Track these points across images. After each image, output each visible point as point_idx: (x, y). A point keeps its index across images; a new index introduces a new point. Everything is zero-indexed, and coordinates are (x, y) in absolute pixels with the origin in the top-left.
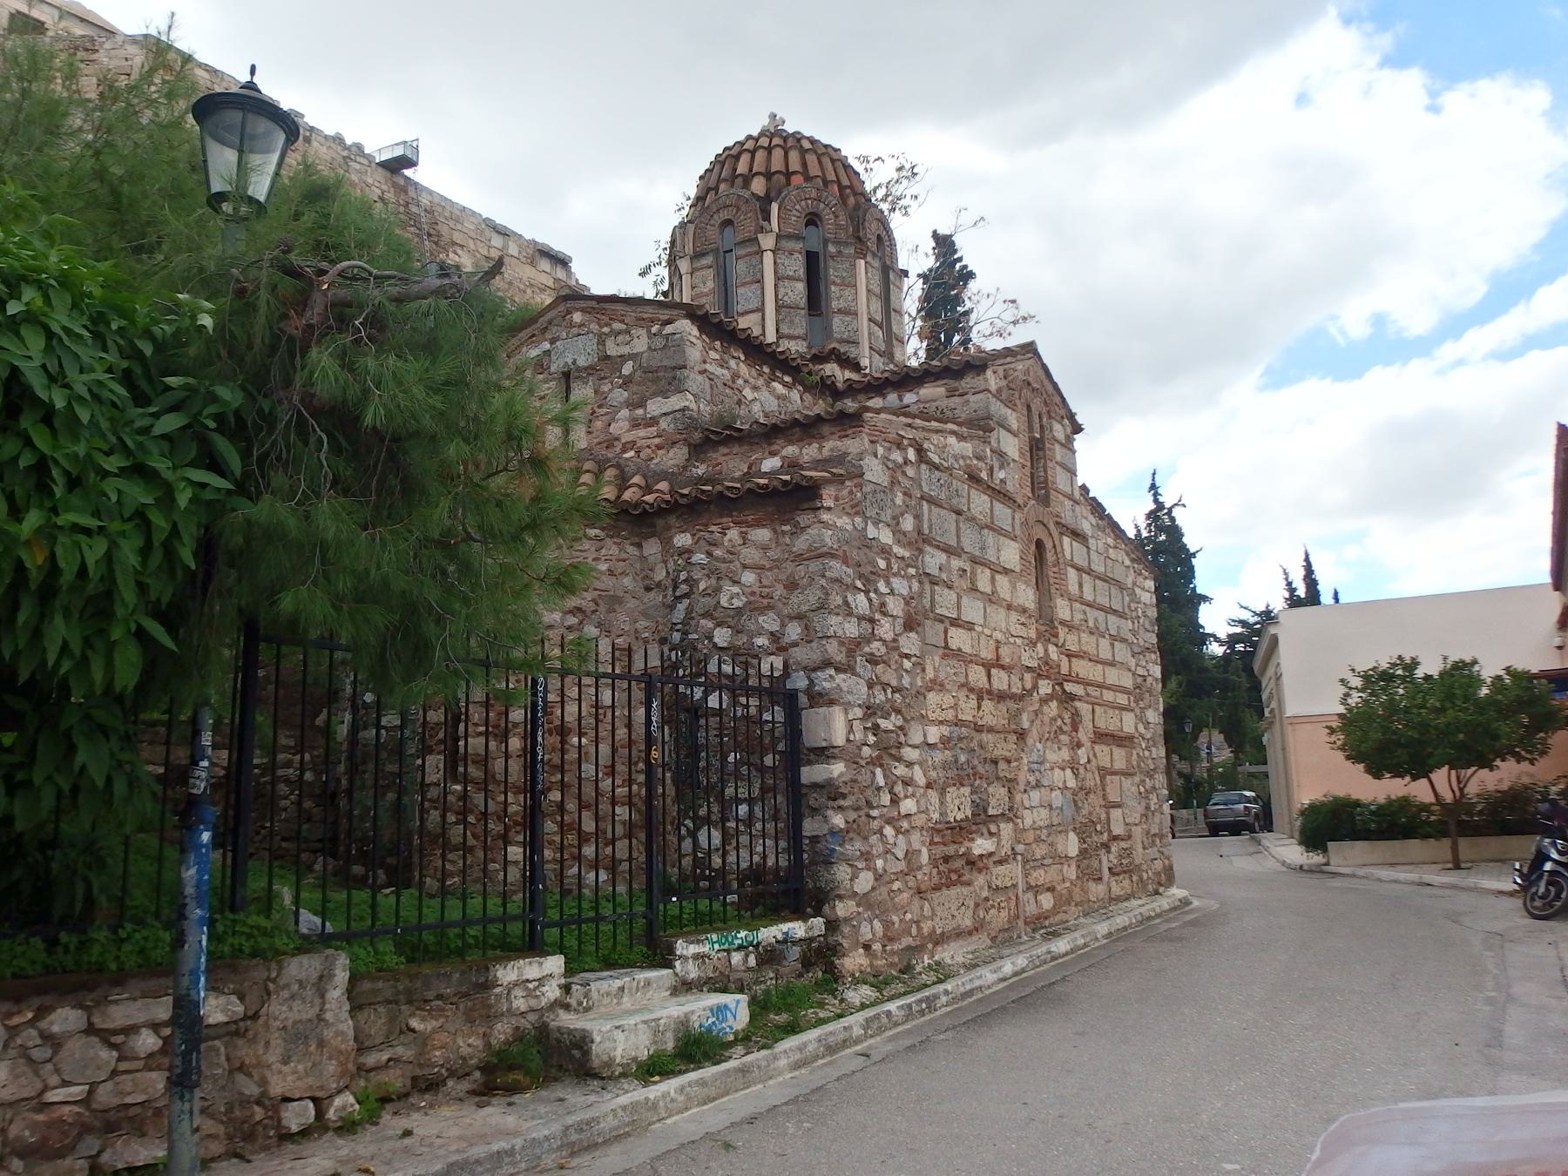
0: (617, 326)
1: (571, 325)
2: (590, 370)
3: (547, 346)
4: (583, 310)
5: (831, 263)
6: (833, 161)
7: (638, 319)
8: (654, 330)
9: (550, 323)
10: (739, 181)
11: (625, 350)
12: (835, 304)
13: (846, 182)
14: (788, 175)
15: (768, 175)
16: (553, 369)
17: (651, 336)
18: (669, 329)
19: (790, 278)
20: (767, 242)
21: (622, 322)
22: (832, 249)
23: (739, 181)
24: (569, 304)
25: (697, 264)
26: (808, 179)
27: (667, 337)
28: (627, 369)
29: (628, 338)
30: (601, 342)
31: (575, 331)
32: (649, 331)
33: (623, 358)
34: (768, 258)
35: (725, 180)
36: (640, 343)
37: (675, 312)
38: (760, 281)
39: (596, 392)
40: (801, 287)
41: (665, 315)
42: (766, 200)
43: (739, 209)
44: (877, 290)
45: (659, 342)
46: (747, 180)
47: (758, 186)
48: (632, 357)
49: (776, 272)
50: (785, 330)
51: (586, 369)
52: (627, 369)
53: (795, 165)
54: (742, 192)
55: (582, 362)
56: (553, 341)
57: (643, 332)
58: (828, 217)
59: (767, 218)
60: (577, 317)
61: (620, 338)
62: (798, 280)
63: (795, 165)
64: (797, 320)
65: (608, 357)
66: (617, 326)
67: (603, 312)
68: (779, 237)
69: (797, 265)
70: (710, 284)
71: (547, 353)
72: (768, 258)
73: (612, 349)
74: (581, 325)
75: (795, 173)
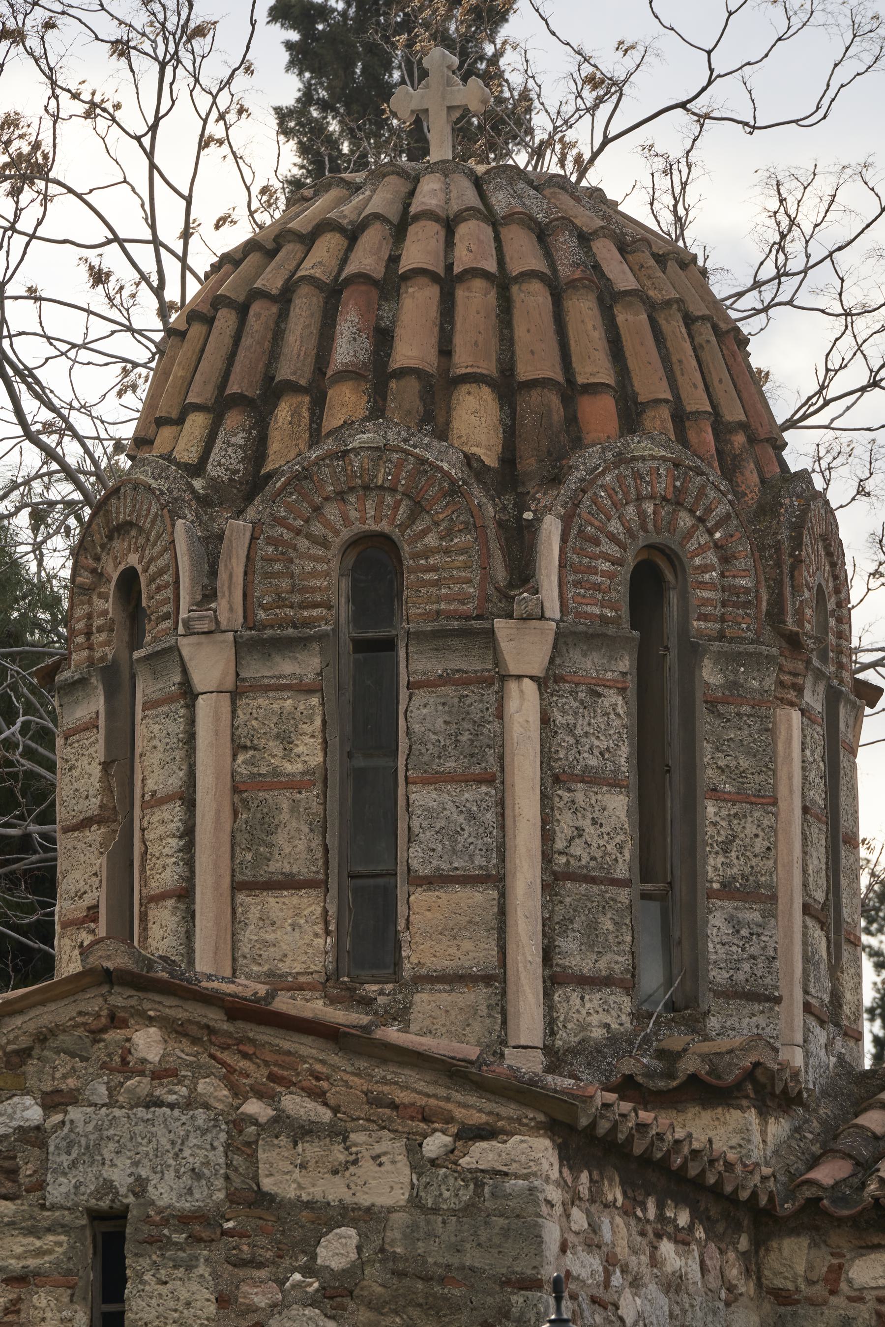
0: (297, 1105)
1: (125, 1065)
2: (199, 1226)
3: (31, 1112)
4: (175, 1030)
5: (705, 722)
6: (689, 320)
7: (376, 1101)
8: (435, 1144)
9: (42, 1038)
10: (405, 395)
11: (333, 1190)
12: (714, 867)
13: (734, 413)
14: (571, 390)
15: (507, 387)
16: (58, 1190)
17: (420, 1165)
18: (482, 1155)
19: (592, 779)
20: (524, 649)
21: (319, 1096)
22: (710, 675)
23: (405, 395)
24: (120, 998)
25: (257, 670)
26: (631, 414)
27: (477, 1178)
28: (337, 1250)
29: (339, 1154)
30: (242, 1139)
31: (139, 1085)
32: (414, 1148)
33: (328, 1217)
34: (523, 706)
35: (347, 374)
36: (385, 1183)
37: (510, 1110)
38: (495, 779)
39: (223, 1301)
40: (618, 806)
41: (473, 1109)
42: (507, 477)
43: (418, 509)
44: (818, 796)
45: (451, 1194)
46: (439, 388)
47: (476, 422)
48: (366, 1218)
49: (547, 757)
50: (575, 956)
51: (184, 1220)
52: (337, 1250)
53: (594, 367)
54: (428, 449)
55: (165, 1193)
56: (53, 1101)
57: (391, 1146)
58: (701, 559)
59: (523, 573)
60: (148, 1043)
61: (310, 1150)
62: (615, 784)
63: (594, 367)
64: (607, 924)
65: (262, 1200)
66: (297, 1105)
67: (238, 1045)
68: (563, 639)
69: (607, 731)
70: (309, 752)
71: (34, 1136)
72: (523, 706)
73: (283, 1175)
74: (162, 1074)
75: (592, 389)
